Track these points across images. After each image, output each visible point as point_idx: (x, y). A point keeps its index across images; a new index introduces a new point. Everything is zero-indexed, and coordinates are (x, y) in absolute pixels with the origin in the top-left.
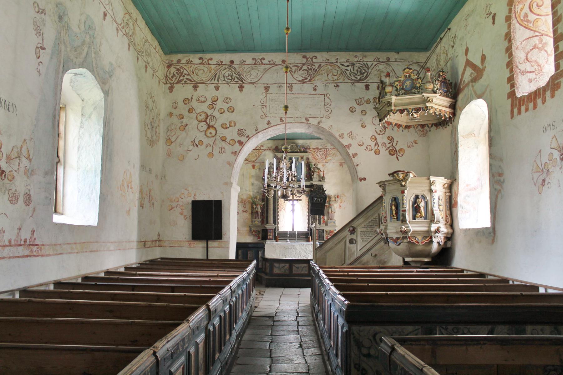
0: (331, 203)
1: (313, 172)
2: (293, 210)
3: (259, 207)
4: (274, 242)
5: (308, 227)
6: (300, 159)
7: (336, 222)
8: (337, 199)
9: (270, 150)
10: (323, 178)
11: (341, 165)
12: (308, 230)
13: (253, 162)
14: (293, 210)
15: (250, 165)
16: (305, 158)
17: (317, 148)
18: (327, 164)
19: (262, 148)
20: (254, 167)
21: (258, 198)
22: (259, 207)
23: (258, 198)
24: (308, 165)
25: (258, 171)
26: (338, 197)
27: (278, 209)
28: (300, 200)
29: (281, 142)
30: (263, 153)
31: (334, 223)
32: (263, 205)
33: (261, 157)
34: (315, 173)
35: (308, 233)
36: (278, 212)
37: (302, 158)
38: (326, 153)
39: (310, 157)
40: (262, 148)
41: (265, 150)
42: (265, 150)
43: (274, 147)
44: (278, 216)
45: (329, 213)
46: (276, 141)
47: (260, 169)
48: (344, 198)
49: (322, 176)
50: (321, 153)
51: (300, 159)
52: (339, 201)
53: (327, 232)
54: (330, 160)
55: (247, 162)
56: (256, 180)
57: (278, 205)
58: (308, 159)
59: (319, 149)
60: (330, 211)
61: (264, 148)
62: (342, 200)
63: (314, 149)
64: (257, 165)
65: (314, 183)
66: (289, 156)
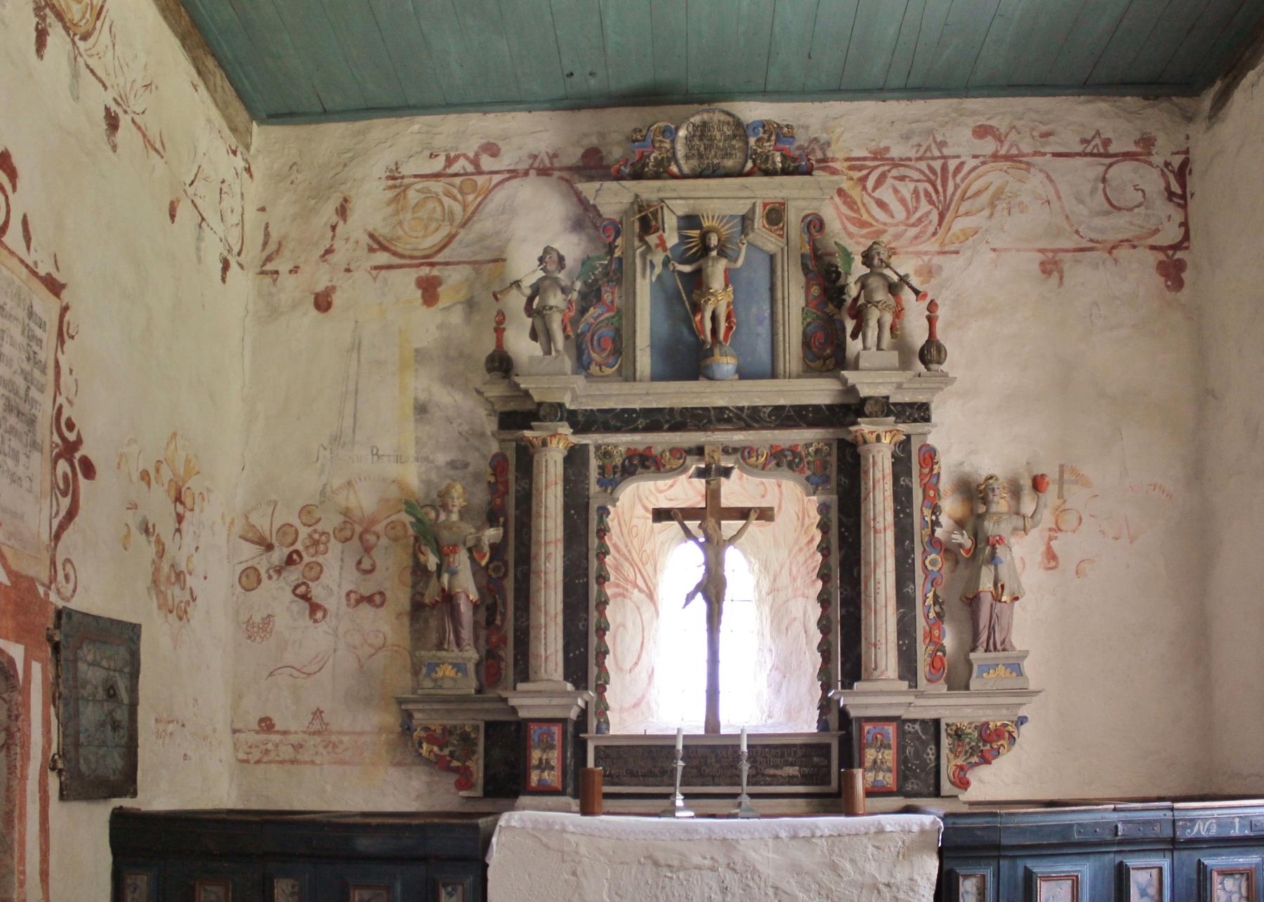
0: (990, 527)
1: (859, 315)
2: (712, 589)
3: (462, 560)
4: (567, 819)
5: (825, 705)
6: (759, 222)
7: (1027, 666)
8: (1028, 506)
9: (544, 172)
10: (931, 353)
11: (1050, 267)
12: (823, 725)
13: (427, 260)
14: (712, 589)
15: (405, 282)
16: (793, 218)
17: (879, 155)
18: (950, 265)
19: (487, 163)
20: (429, 290)
21: (458, 498)
22: (462, 560)
23: (458, 498)
24: (825, 275)
25: (456, 317)
26: (1038, 484)
27: (602, 578)
28: (765, 514)
29: (623, 121)
30: (499, 197)
31: (1016, 668)
32: (497, 550)
33: (484, 225)
34: (873, 315)
35: (823, 749)
36: (603, 603)
37: (775, 215)
38: (941, 188)
39: (832, 214)
40: (487, 163)
41: (514, 174)
42: (514, 174)
43: (573, 156)
44: (602, 629)
45: (972, 602)
46: (585, 116)
47: (471, 305)
48: (1077, 497)
49: (919, 337)
50: (906, 189)
51: (759, 222)
52: (1047, 518)
53: (958, 735)
54: (967, 234)
55: (383, 258)
56: (448, 380)
57: (603, 552)
58: (815, 224)
59: (895, 164)
60: (986, 584)
61: (506, 161)
62: (1060, 512)
63: (855, 164)
64: (454, 278)
65: (868, 384)
66: (681, 208)
